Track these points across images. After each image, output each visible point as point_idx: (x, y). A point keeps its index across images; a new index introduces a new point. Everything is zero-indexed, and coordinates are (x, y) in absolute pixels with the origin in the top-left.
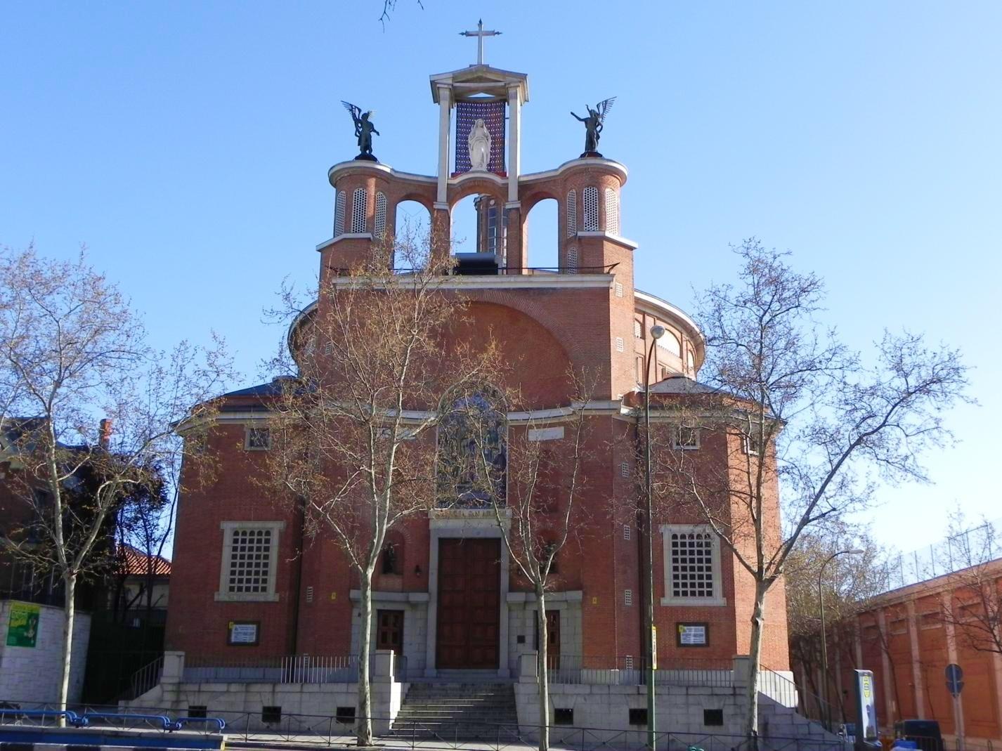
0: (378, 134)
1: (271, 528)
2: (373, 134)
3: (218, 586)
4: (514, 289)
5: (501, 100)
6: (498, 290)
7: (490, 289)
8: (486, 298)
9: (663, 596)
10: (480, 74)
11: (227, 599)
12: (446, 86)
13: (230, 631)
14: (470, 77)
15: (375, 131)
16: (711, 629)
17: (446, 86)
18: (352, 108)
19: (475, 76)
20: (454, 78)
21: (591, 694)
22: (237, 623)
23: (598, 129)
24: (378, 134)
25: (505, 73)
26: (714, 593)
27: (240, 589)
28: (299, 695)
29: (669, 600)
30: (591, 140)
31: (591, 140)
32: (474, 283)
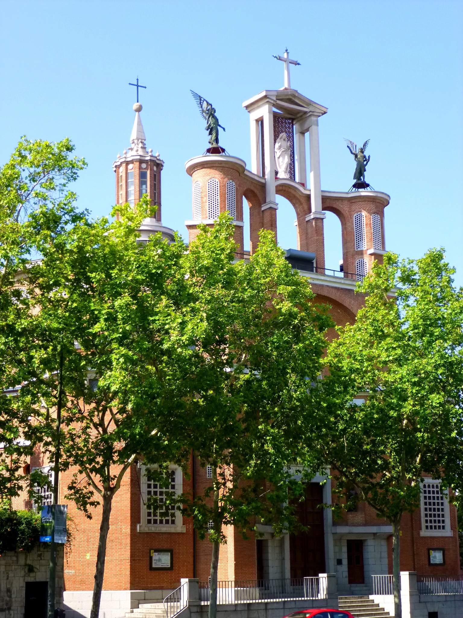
0: (224, 129)
1: (176, 469)
2: (218, 127)
3: (139, 518)
4: (342, 289)
5: (290, 119)
6: (333, 287)
7: (327, 286)
8: (325, 293)
9: (421, 529)
10: (291, 97)
11: (146, 530)
12: (272, 102)
13: (151, 558)
14: (284, 97)
15: (220, 126)
16: (446, 552)
17: (272, 102)
18: (200, 100)
19: (288, 97)
20: (277, 96)
21: (446, 601)
22: (156, 551)
23: (365, 163)
24: (224, 129)
25: (309, 103)
26: (446, 527)
27: (155, 522)
28: (283, 610)
29: (424, 533)
30: (360, 172)
31: (360, 172)
32: (318, 279)
